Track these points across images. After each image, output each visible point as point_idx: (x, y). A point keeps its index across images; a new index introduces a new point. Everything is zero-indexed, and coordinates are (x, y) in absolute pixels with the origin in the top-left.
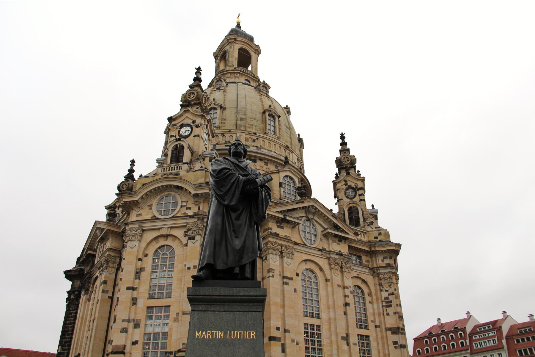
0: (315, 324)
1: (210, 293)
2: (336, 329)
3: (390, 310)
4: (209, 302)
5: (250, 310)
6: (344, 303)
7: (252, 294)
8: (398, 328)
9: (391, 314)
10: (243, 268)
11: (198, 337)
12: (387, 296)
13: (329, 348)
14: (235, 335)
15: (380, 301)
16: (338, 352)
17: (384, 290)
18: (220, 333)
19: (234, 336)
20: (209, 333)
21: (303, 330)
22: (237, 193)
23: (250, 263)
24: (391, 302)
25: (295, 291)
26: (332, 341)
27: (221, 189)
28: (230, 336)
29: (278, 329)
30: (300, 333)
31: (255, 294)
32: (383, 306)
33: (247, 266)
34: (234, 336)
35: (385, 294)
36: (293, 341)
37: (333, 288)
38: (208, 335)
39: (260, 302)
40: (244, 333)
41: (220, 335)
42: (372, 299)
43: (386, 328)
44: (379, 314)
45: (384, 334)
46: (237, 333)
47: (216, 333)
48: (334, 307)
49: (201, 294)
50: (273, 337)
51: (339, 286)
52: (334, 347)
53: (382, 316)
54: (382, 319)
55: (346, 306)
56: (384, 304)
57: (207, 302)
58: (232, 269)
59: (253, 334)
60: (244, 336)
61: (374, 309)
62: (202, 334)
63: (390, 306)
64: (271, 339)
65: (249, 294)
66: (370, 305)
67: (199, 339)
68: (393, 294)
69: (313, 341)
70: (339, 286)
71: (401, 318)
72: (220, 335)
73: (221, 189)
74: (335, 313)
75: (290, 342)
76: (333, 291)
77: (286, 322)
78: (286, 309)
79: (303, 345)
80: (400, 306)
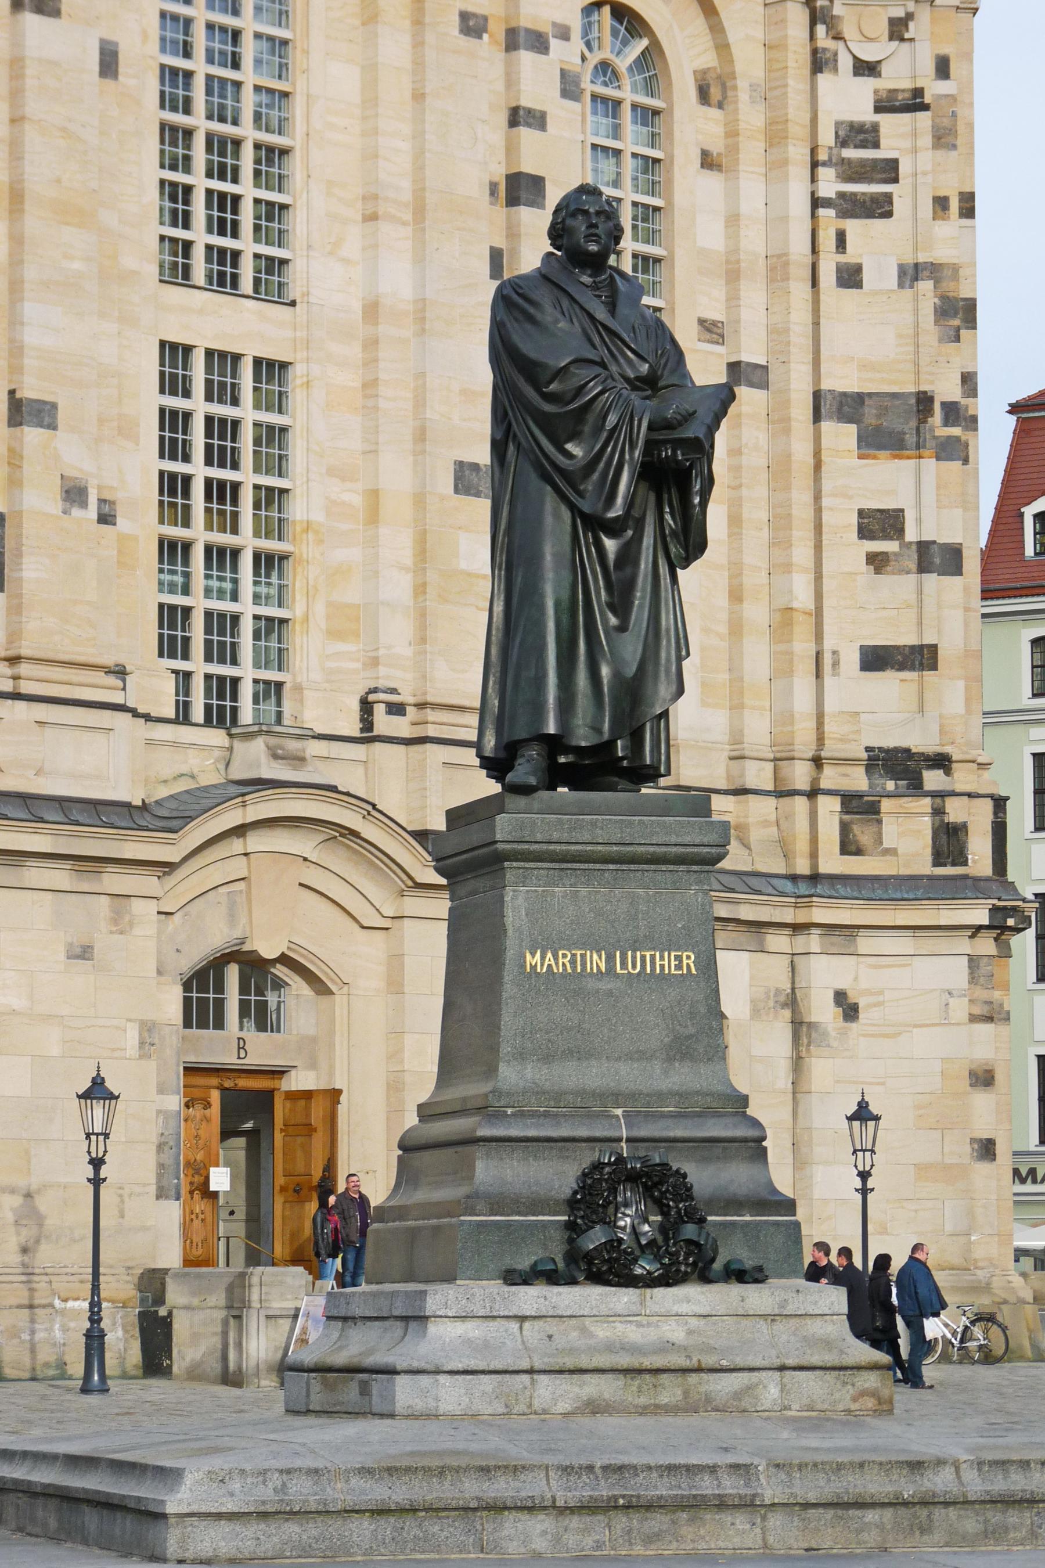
0: (250, 350)
1: (565, 837)
2: (420, 402)
3: (875, 245)
6: (499, 172)
7: (687, 839)
8: (924, 401)
9: (881, 274)
10: (636, 737)
11: (533, 968)
12: (865, 113)
13: (351, 554)
14: (633, 963)
15: (798, 153)
16: (420, 589)
17: (845, 63)
18: (595, 957)
19: (634, 967)
20: (564, 956)
21: (149, 401)
22: (626, 468)
24: (890, 171)
25: (109, 63)
26: (374, 496)
27: (569, 446)
30: (127, 430)
31: (697, 841)
32: (816, 203)
33: (648, 726)
34: (634, 967)
35: (847, 98)
36: (74, 494)
37: (418, 44)
38: (562, 962)
40: (662, 958)
41: (597, 961)
42: (732, 133)
43: (817, 395)
44: (777, 268)
45: (801, 450)
46: (643, 958)
47: (583, 956)
48: (420, 210)
49: (539, 837)
51: (472, 25)
52: (397, 544)
53: (800, 290)
54: (800, 316)
55: (513, 200)
56: (829, 185)
57: (553, 861)
58: (611, 744)
59: (689, 959)
60: (662, 967)
61: (733, 220)
62: (543, 958)
63: (879, 208)
65: (680, 840)
66: (712, 180)
68: (915, 102)
69: (221, 493)
70: (472, 25)
71: (959, 314)
73: (569, 446)
74: (420, 258)
75: (53, 504)
76: (419, 65)
77: (31, 337)
78: (33, 223)
79: (143, 524)
80: (968, 211)
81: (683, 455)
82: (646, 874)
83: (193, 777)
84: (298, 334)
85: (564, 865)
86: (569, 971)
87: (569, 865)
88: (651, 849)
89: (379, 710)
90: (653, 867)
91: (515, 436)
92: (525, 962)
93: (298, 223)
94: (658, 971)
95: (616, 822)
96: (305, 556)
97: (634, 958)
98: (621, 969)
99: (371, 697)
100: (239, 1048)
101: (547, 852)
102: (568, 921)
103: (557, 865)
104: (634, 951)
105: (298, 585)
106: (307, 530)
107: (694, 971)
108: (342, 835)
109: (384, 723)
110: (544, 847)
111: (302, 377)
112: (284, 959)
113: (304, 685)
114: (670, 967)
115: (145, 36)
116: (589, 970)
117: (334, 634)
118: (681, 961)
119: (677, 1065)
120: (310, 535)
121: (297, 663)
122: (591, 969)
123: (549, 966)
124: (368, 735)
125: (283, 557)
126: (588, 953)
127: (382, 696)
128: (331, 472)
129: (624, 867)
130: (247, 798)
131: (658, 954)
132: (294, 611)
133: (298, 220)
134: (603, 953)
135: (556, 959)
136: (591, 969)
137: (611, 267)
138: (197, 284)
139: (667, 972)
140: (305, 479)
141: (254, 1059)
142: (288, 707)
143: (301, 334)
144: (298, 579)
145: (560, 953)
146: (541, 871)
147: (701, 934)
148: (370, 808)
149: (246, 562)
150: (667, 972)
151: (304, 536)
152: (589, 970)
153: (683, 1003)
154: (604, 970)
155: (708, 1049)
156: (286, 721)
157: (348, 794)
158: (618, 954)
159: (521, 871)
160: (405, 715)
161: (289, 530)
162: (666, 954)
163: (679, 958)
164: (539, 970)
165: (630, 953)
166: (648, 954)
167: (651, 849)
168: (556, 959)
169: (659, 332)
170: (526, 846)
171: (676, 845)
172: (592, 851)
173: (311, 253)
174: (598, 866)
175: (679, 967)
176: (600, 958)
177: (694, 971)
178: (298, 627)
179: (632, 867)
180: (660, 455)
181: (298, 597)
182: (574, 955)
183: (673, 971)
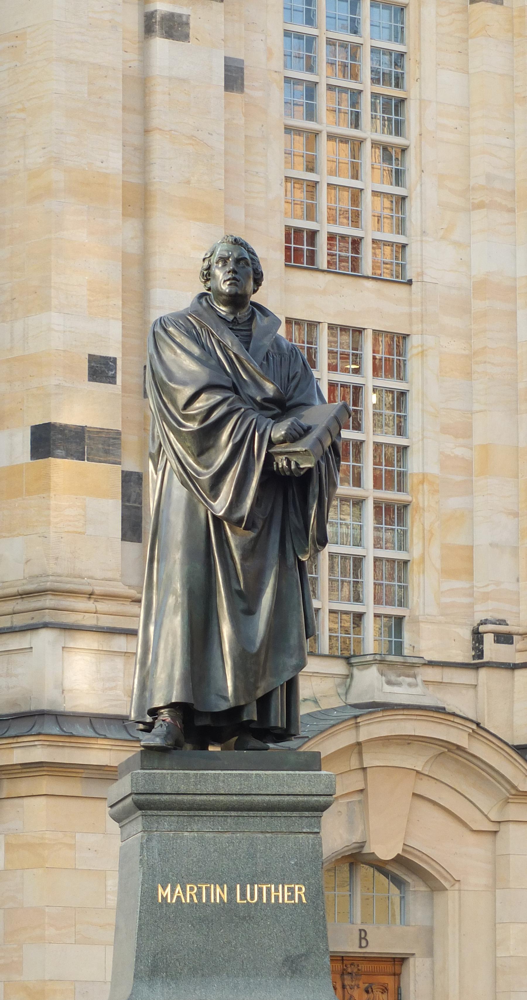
0: (370, 324)
1: (192, 789)
5: (292, 829)
7: (298, 790)
10: (264, 703)
11: (164, 899)
18: (218, 890)
19: (252, 897)
20: (192, 889)
23: (282, 686)
29: (101, 369)
34: (252, 897)
40: (277, 890)
41: (219, 894)
46: (260, 891)
47: (208, 889)
49: (168, 790)
50: (62, 429)
57: (182, 809)
59: (300, 891)
60: (277, 897)
62: (173, 891)
64: (46, 440)
65: (291, 791)
67: (168, 905)
72: (219, 894)
81: (297, 464)
82: (264, 819)
83: (316, 702)
84: (414, 309)
85: (191, 813)
86: (196, 901)
87: (197, 813)
88: (267, 798)
89: (488, 639)
90: (269, 814)
91: (164, 451)
92: (157, 894)
93: (414, 211)
94: (273, 901)
95: (236, 775)
96: (421, 505)
97: (252, 891)
98: (241, 899)
99: (482, 629)
100: (361, 939)
101: (175, 802)
102: (195, 859)
105: (415, 530)
106: (422, 482)
107: (304, 901)
108: (449, 750)
109: (492, 650)
110: (174, 797)
111: (418, 346)
112: (399, 860)
113: (421, 618)
114: (283, 897)
115: (269, 53)
116: (212, 901)
117: (448, 573)
119: (288, 980)
120: (426, 486)
121: (415, 599)
122: (215, 899)
123: (178, 897)
124: (477, 663)
125: (405, 506)
126: (212, 886)
127: (490, 627)
128: (445, 430)
129: (245, 813)
130: (359, 720)
131: (273, 886)
132: (415, 552)
133: (413, 210)
134: (225, 886)
136: (215, 899)
137: (254, 304)
138: (321, 268)
139: (281, 901)
140: (420, 437)
141: (375, 947)
142: (407, 637)
143: (416, 309)
144: (416, 526)
145: (188, 886)
146: (173, 818)
147: (312, 869)
148: (474, 727)
149: (369, 509)
150: (281, 901)
151: (421, 487)
152: (212, 901)
153: (294, 927)
154: (226, 901)
156: (406, 652)
157: (454, 714)
158: (238, 886)
159: (155, 818)
160: (512, 643)
161: (410, 482)
162: (281, 886)
163: (291, 890)
164: (169, 901)
165: (248, 886)
166: (264, 887)
167: (267, 798)
169: (293, 359)
170: (157, 797)
171: (288, 795)
172: (216, 801)
173: (424, 238)
174: (221, 813)
175: (291, 897)
176: (223, 891)
177: (304, 901)
178: (415, 568)
179: (251, 814)
180: (277, 464)
181: (415, 540)
182: (200, 889)
183: (286, 901)
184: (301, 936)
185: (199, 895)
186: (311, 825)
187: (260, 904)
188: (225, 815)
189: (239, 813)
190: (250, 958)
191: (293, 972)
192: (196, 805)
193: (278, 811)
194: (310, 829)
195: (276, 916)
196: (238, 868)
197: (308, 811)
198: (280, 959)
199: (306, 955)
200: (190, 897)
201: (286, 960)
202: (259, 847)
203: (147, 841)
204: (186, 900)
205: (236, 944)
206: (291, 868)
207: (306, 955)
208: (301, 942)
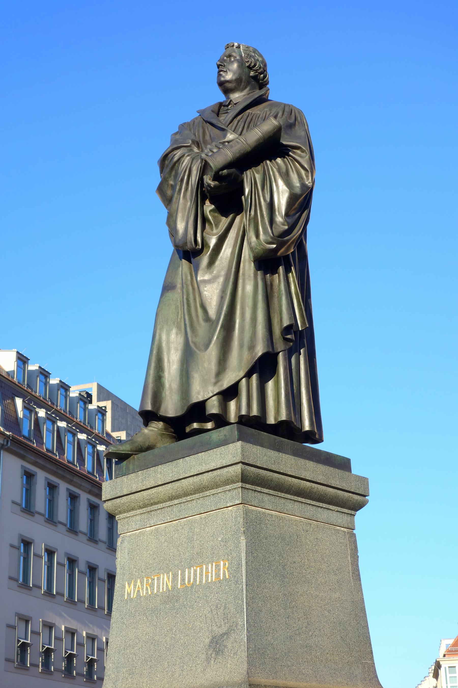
4: (145, 506)
11: (129, 595)
28: (183, 580)
39: (233, 482)
47: (158, 579)
57: (140, 508)
62: (135, 587)
82: (199, 501)
85: (149, 509)
92: (125, 592)
103: (145, 510)
104: (189, 568)
118: (220, 569)
123: (138, 591)
129: (184, 499)
134: (171, 573)
135: (142, 585)
153: (219, 606)
155: (235, 644)
158: (180, 572)
162: (210, 565)
165: (187, 570)
168: (142, 585)
174: (168, 504)
176: (169, 579)
179: (188, 498)
184: (224, 614)
185: (152, 586)
186: (233, 498)
187: (195, 587)
188: (170, 504)
189: (180, 500)
190: (185, 643)
191: (217, 653)
192: (146, 500)
193: (206, 490)
194: (232, 502)
195: (206, 596)
196: (180, 554)
197: (228, 484)
198: (207, 641)
199: (227, 634)
200: (146, 590)
201: (211, 642)
202: (196, 529)
203: (121, 543)
204: (143, 594)
205: (176, 631)
206: (219, 545)
207: (227, 634)
208: (224, 620)
